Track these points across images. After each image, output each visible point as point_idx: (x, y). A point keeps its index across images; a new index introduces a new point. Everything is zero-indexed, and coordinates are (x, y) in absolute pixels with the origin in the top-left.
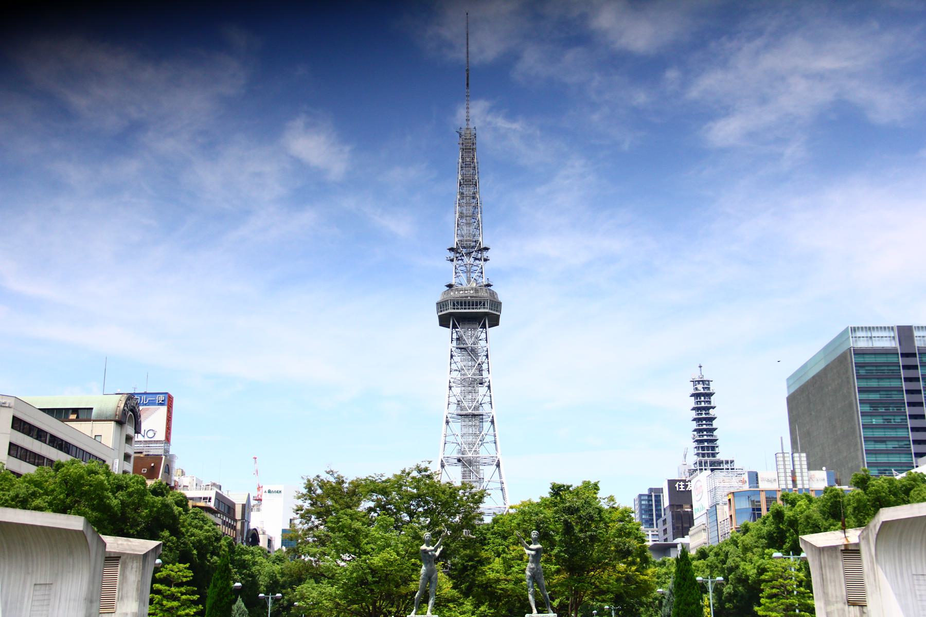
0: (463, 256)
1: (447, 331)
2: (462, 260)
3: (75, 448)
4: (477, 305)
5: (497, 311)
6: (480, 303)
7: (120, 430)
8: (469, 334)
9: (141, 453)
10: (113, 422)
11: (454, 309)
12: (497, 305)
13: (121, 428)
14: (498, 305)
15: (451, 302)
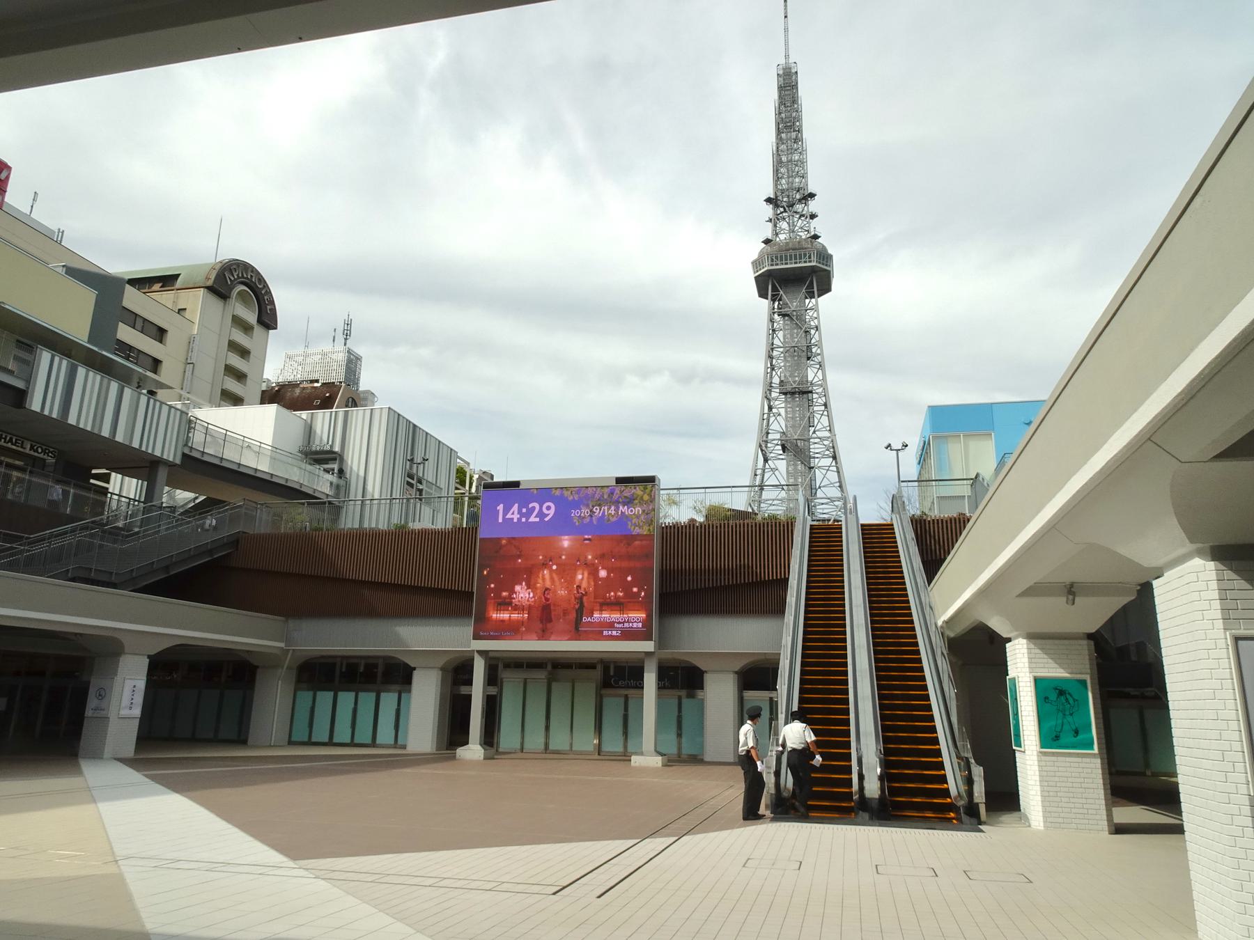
0: (785, 211)
1: (765, 303)
2: (784, 219)
3: (134, 316)
4: (800, 258)
5: (826, 265)
6: (805, 255)
7: (223, 304)
8: (793, 302)
9: (317, 381)
10: (202, 289)
11: (772, 265)
12: (825, 257)
13: (225, 304)
14: (827, 258)
15: (768, 257)
